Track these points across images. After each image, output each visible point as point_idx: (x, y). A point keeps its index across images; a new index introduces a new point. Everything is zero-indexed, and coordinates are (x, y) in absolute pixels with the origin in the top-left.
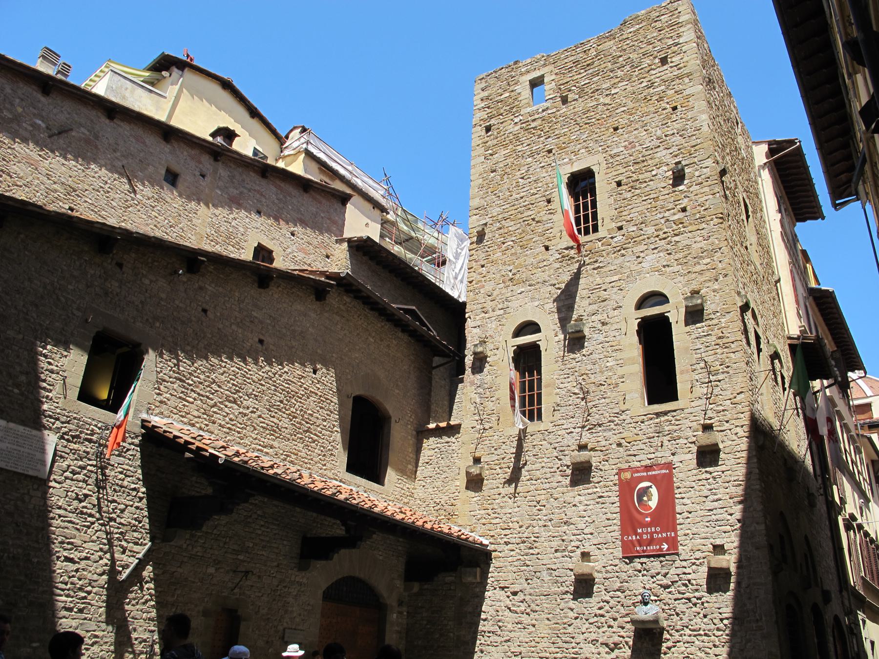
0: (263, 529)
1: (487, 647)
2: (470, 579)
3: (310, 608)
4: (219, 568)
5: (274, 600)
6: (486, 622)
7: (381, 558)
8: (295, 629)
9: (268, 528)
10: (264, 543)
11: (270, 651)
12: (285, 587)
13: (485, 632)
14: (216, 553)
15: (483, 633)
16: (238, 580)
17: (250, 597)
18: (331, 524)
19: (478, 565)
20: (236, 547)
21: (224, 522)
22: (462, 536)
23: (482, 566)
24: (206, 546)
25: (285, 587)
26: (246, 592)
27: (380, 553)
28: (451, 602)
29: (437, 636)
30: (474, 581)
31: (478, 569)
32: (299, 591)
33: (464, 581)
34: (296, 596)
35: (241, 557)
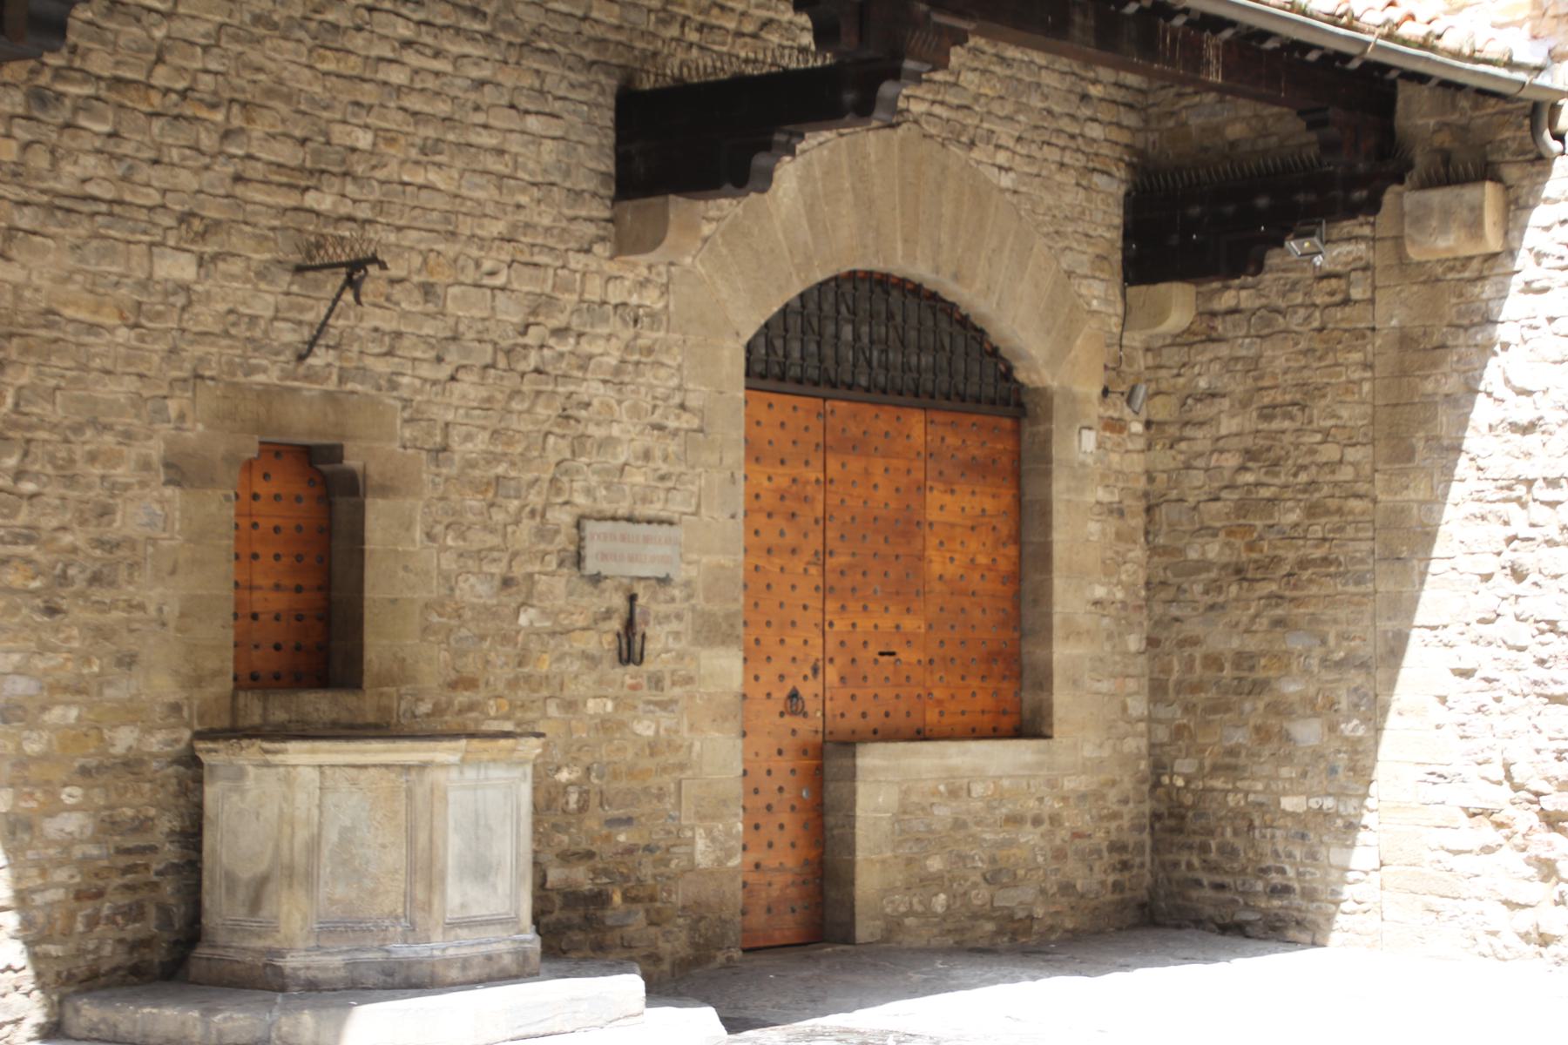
0: (411, 57)
1: (1545, 551)
2: (1448, 243)
3: (688, 421)
4: (216, 257)
5: (516, 393)
6: (1533, 440)
7: (1006, 180)
8: (630, 519)
9: (437, 54)
10: (430, 132)
11: (523, 620)
12: (560, 332)
13: (1530, 483)
14: (186, 179)
15: (1521, 490)
16: (324, 311)
17: (394, 386)
18: (749, 28)
19: (1486, 172)
20: (286, 153)
21: (202, 28)
22: (1407, 30)
23: (1511, 173)
24: (127, 148)
25: (560, 332)
26: (369, 361)
27: (1002, 158)
28: (1356, 356)
29: (1293, 517)
30: (1467, 250)
31: (1490, 190)
32: (628, 348)
33: (1414, 253)
34: (617, 371)
35: (323, 201)
